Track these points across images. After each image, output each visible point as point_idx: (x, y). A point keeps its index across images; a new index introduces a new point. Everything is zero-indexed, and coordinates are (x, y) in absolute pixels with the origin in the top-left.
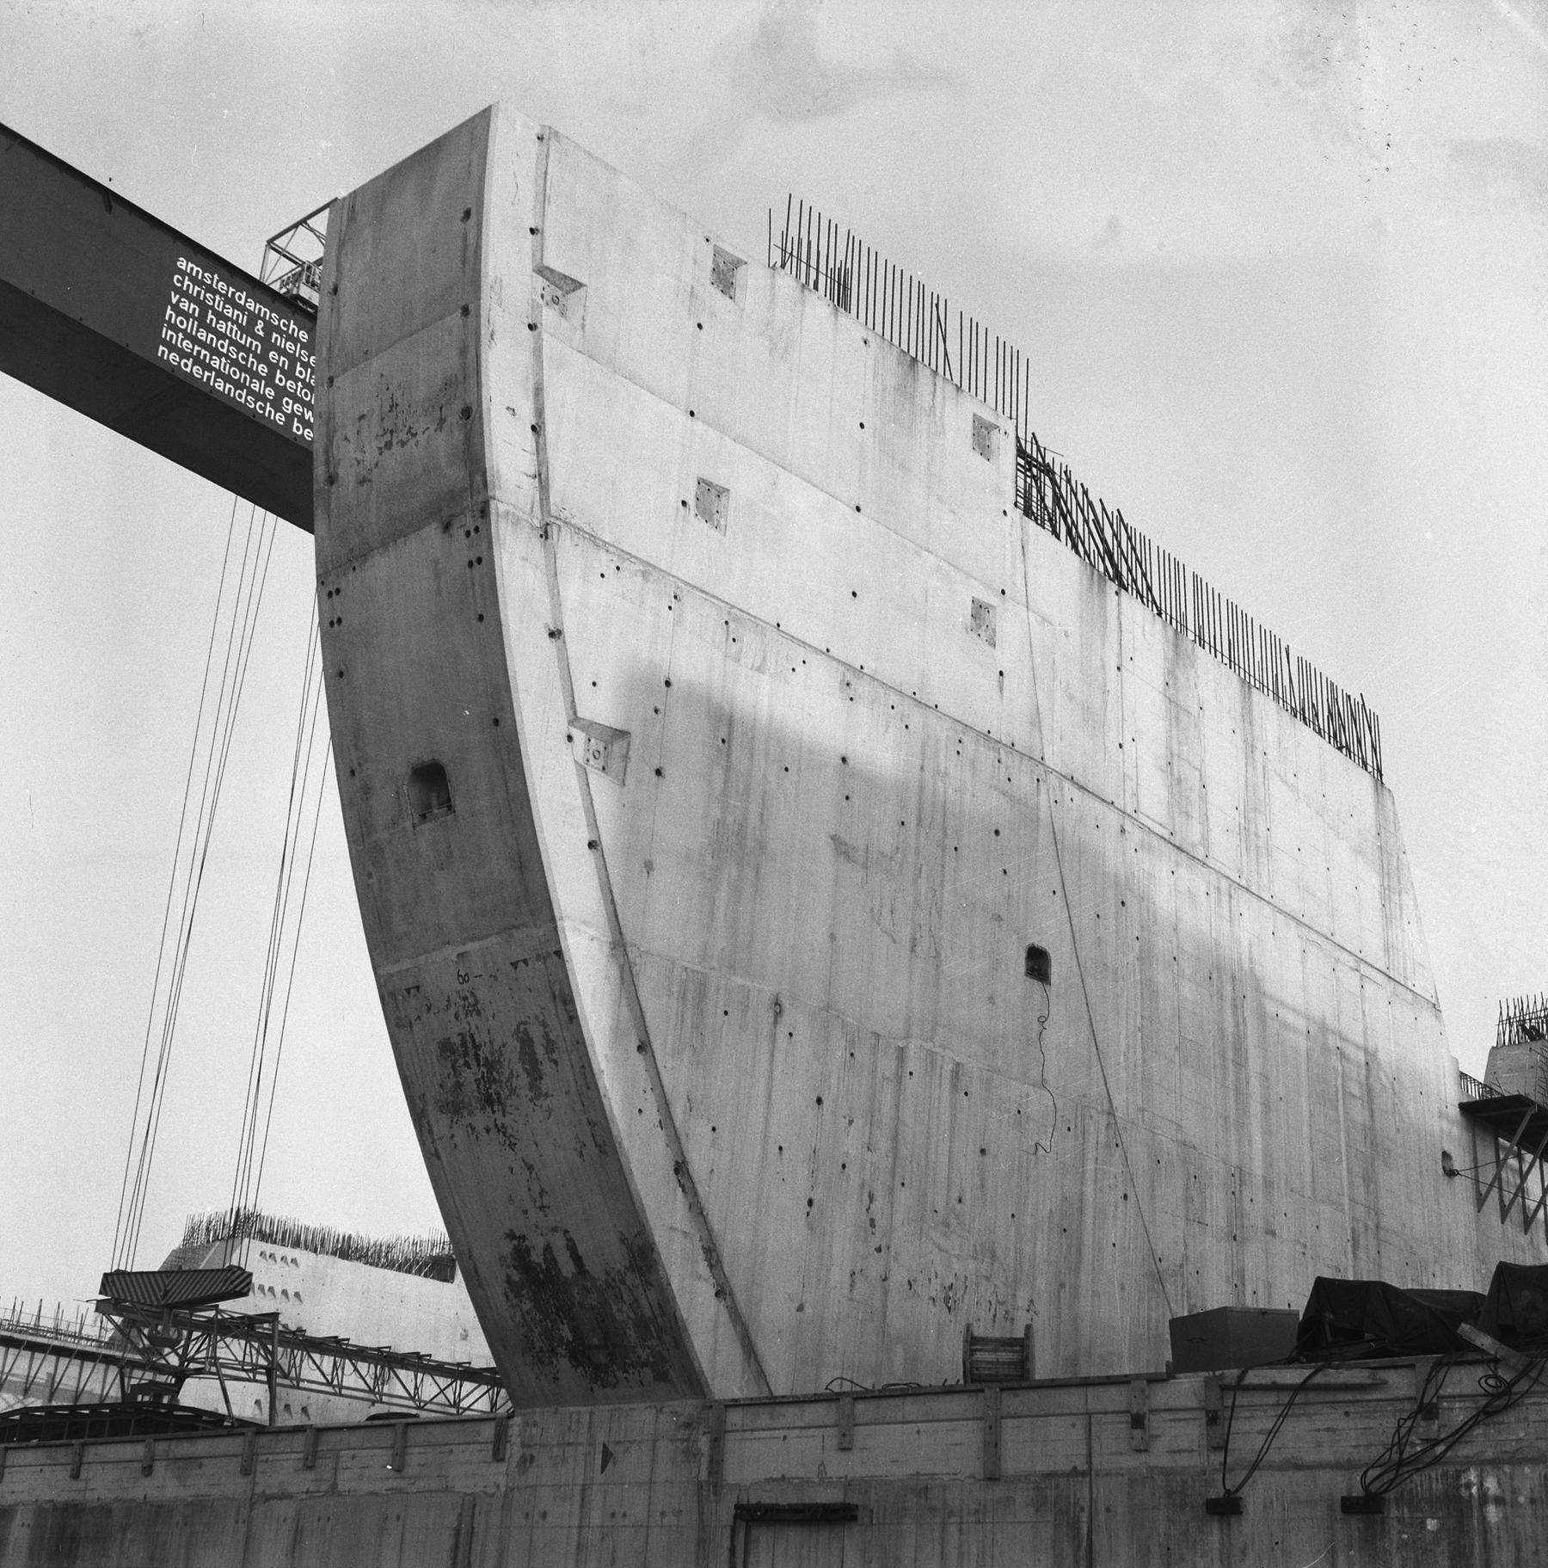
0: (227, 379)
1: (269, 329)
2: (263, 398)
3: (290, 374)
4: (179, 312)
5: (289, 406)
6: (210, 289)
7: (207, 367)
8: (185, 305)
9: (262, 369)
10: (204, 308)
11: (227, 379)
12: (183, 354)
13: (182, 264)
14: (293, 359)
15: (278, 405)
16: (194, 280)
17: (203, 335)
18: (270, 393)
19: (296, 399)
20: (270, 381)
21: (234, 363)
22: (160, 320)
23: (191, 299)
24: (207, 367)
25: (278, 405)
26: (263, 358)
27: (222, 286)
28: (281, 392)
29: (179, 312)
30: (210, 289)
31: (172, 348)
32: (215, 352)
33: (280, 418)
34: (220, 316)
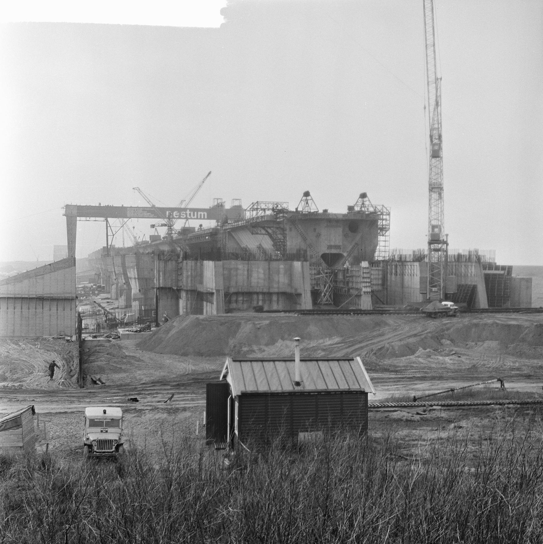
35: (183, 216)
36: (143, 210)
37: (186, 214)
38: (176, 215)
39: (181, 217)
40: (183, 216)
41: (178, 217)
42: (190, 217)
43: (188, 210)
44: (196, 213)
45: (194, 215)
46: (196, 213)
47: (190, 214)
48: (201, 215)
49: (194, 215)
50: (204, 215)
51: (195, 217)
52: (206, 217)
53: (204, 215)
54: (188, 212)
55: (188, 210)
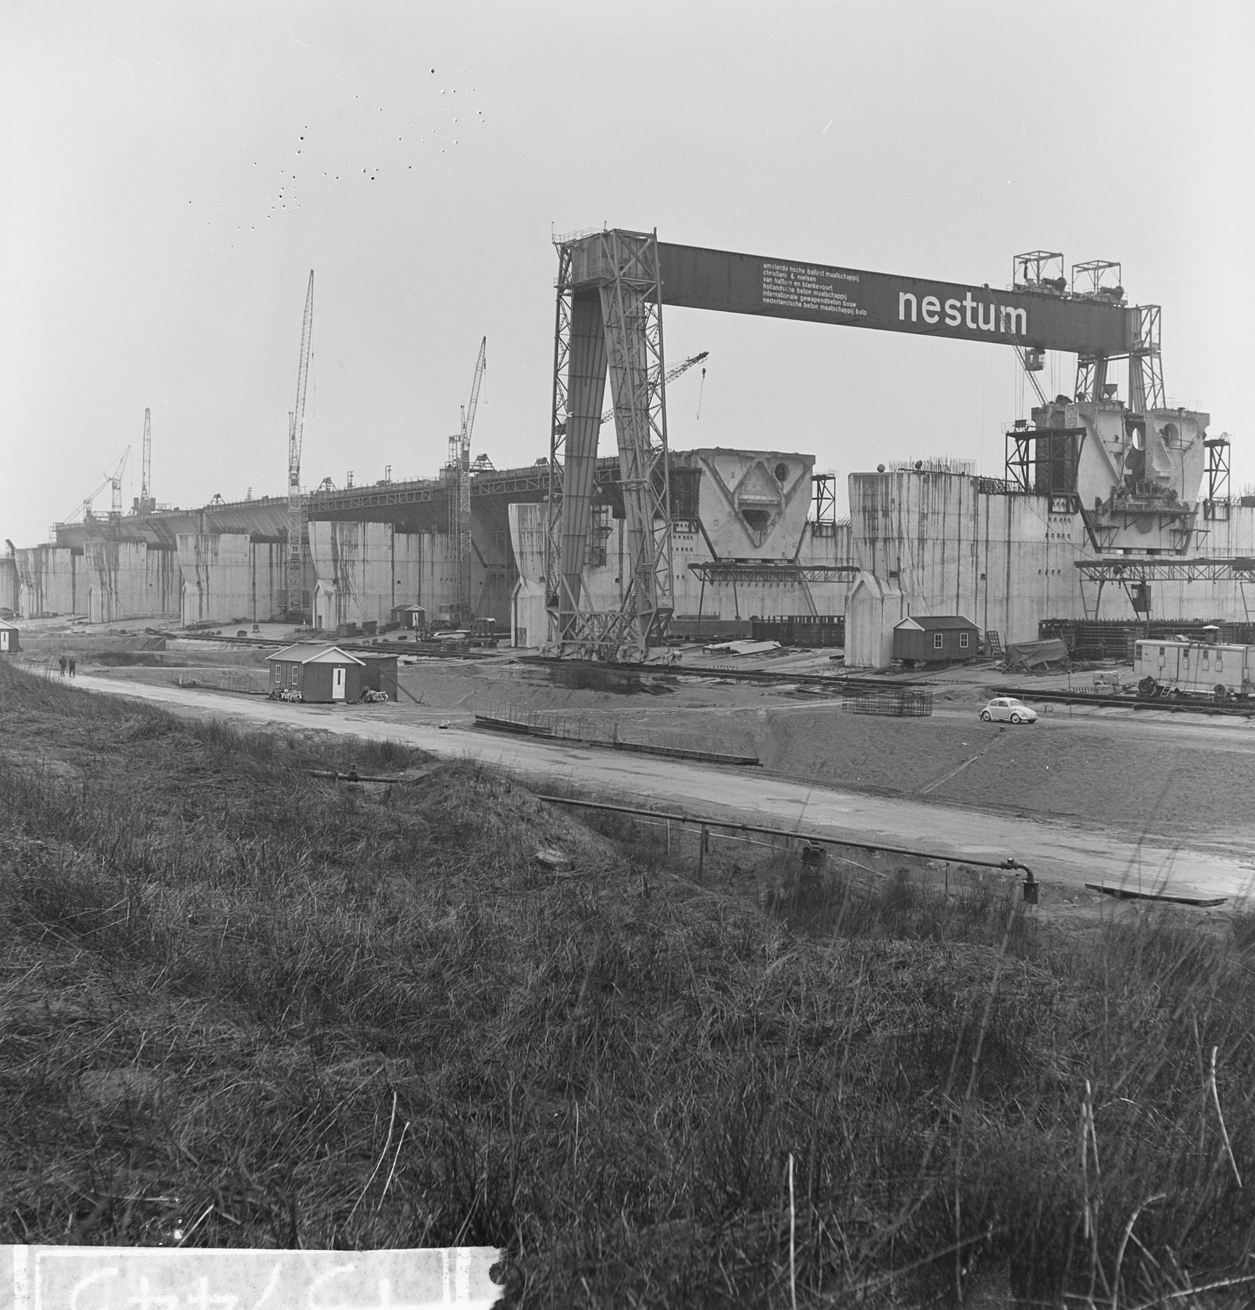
0: (783, 299)
1: (796, 275)
2: (794, 300)
3: (801, 288)
4: (767, 283)
5: (803, 299)
6: (775, 271)
7: (776, 298)
8: (769, 280)
9: (793, 290)
10: (773, 277)
11: (783, 299)
12: (770, 298)
13: (765, 266)
14: (801, 281)
15: (799, 301)
16: (769, 270)
17: (775, 288)
18: (796, 297)
19: (804, 295)
20: (795, 293)
21: (785, 293)
22: (761, 289)
23: (769, 277)
24: (776, 298)
25: (799, 301)
26: (793, 286)
27: (778, 267)
28: (799, 295)
29: (767, 283)
30: (775, 271)
31: (767, 297)
32: (778, 292)
33: (800, 305)
34: (779, 278)
35: (954, 318)
36: (820, 280)
37: (962, 310)
38: (931, 314)
39: (948, 321)
40: (954, 318)
41: (936, 319)
42: (973, 326)
43: (969, 295)
44: (992, 307)
45: (987, 321)
46: (992, 307)
47: (975, 311)
48: (1008, 315)
49: (987, 321)
50: (1019, 317)
51: (991, 326)
52: (1024, 332)
53: (1019, 317)
54: (969, 303)
55: (969, 295)
